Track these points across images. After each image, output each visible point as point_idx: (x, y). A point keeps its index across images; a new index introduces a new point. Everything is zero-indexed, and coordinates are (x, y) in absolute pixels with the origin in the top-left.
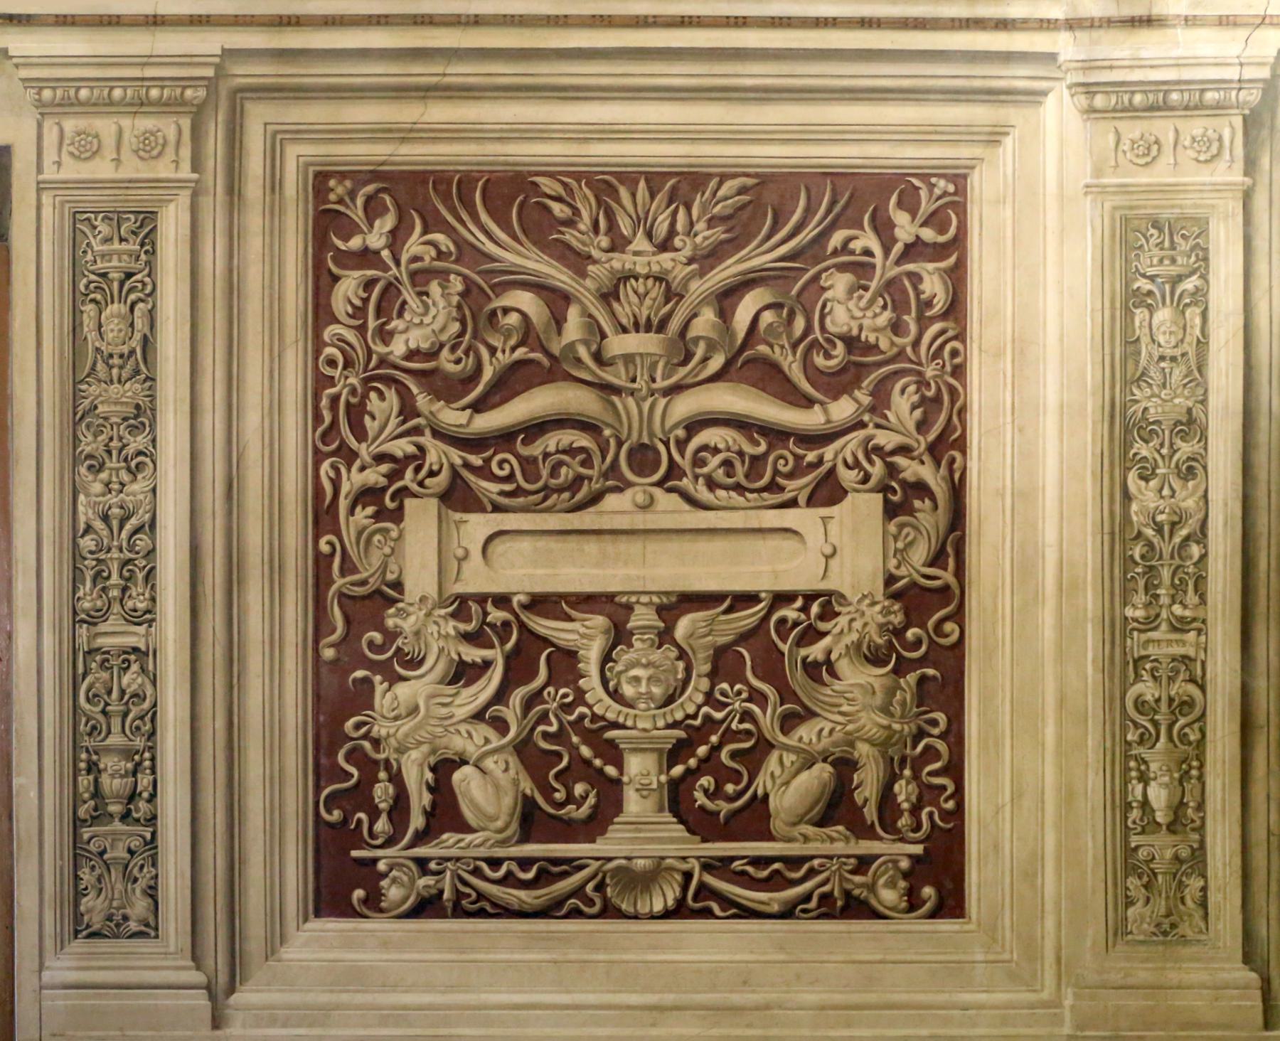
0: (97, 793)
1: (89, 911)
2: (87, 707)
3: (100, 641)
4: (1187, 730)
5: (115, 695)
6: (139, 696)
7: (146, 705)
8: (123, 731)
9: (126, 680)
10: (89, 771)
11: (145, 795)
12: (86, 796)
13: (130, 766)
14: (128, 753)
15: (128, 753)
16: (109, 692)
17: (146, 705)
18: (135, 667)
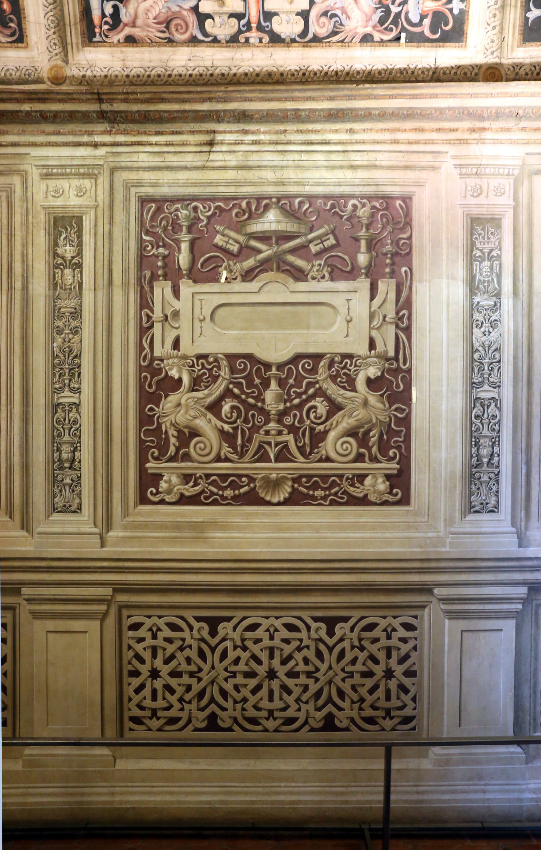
0: (60, 460)
1: (57, 503)
2: (57, 426)
3: (61, 401)
4: (494, 427)
5: (67, 421)
6: (75, 422)
7: (78, 426)
8: (70, 435)
9: (71, 415)
10: (57, 451)
11: (78, 460)
12: (56, 460)
13: (72, 449)
14: (72, 444)
15: (72, 444)
16: (65, 420)
17: (78, 426)
18: (74, 410)
